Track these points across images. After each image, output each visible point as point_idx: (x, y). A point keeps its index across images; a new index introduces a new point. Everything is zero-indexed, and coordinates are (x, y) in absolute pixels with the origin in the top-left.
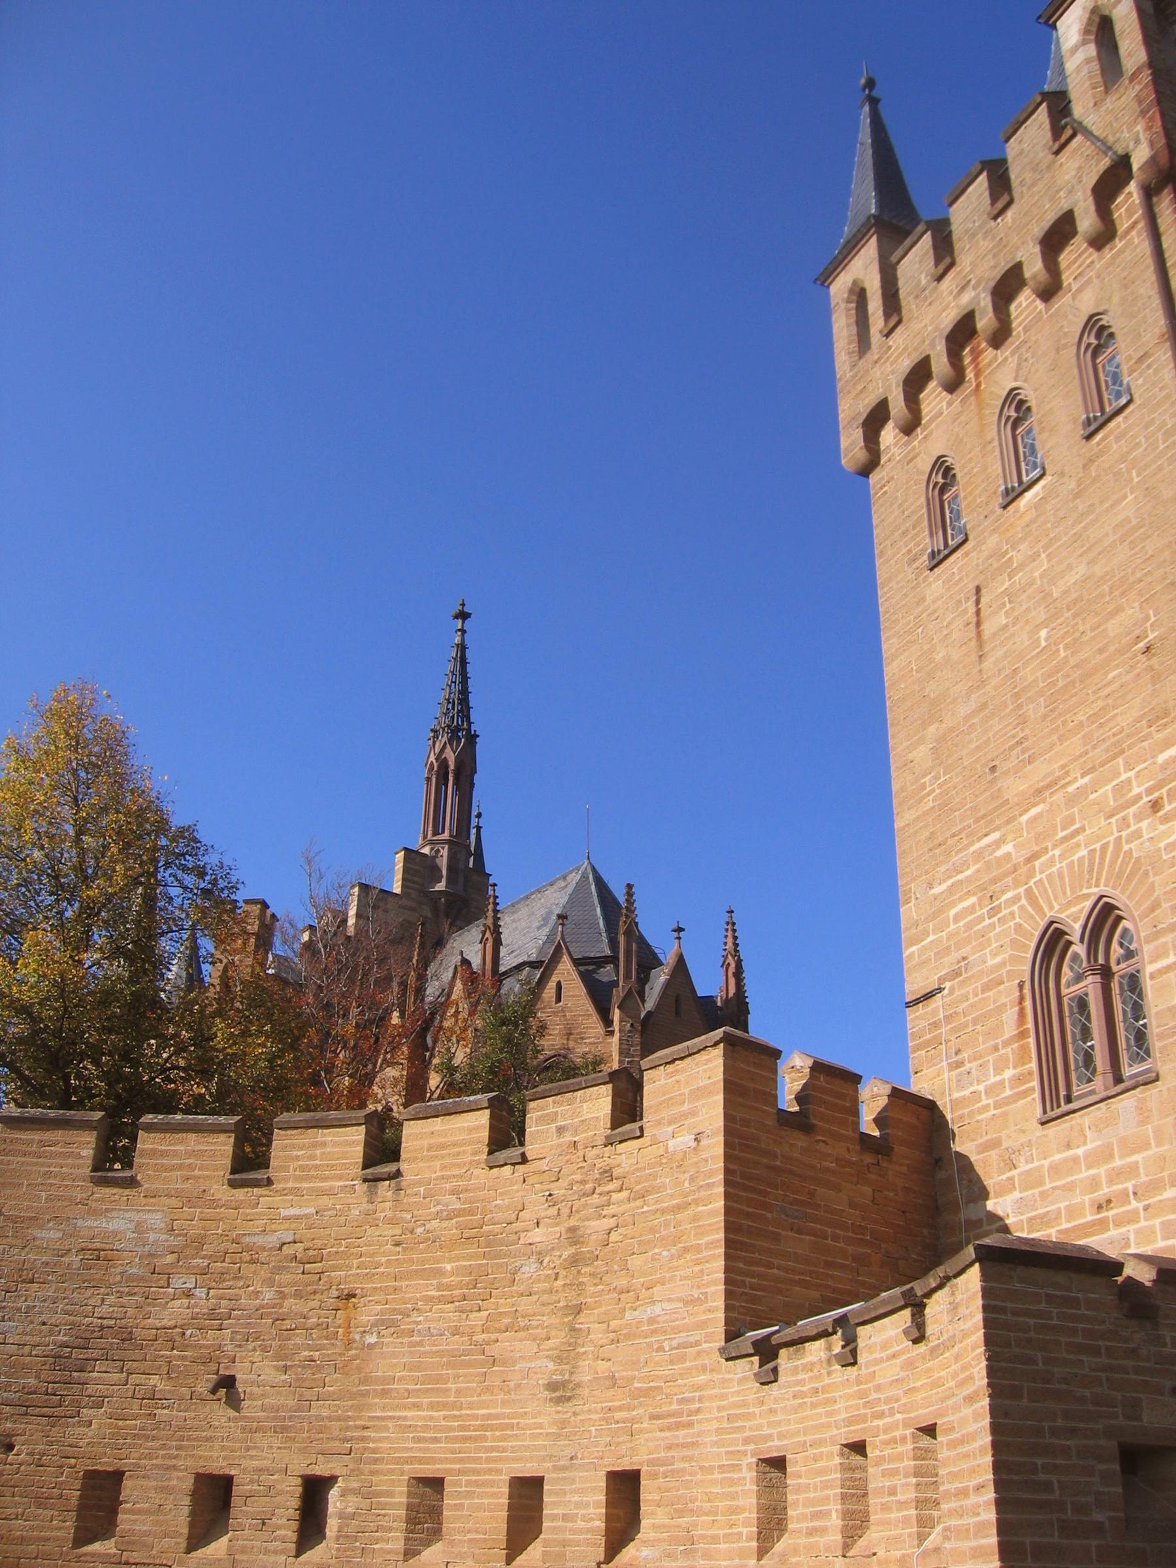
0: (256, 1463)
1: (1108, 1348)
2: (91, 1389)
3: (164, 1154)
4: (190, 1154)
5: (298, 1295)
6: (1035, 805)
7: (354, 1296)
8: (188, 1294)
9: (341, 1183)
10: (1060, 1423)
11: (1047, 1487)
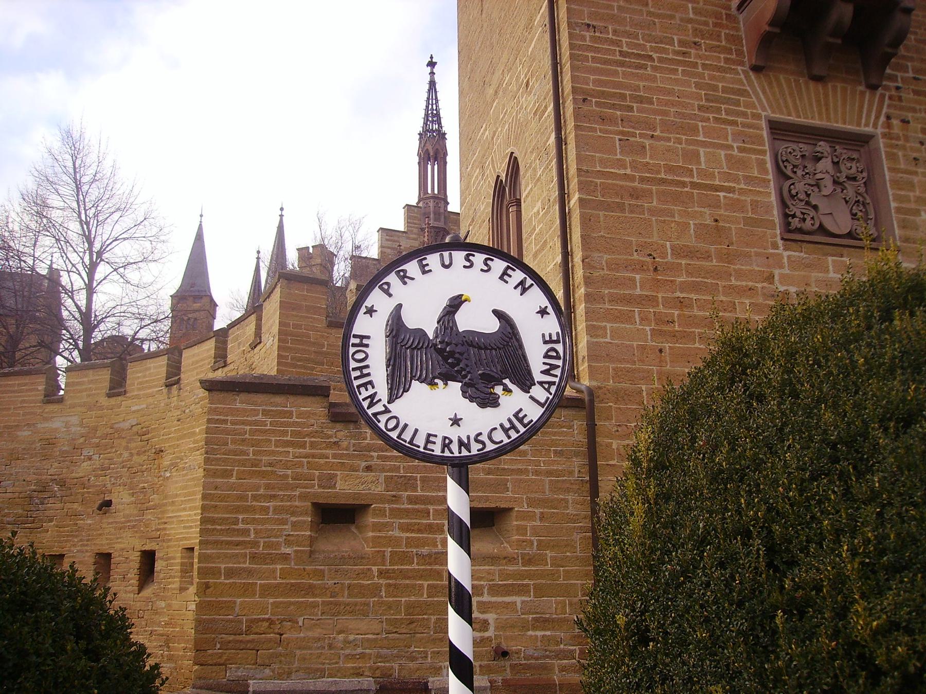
0: (122, 546)
1: (311, 442)
2: (47, 513)
3: (78, 384)
4: (91, 382)
5: (138, 454)
6: (494, 101)
7: (162, 451)
8: (90, 459)
9: (157, 389)
10: (262, 491)
11: (246, 532)
